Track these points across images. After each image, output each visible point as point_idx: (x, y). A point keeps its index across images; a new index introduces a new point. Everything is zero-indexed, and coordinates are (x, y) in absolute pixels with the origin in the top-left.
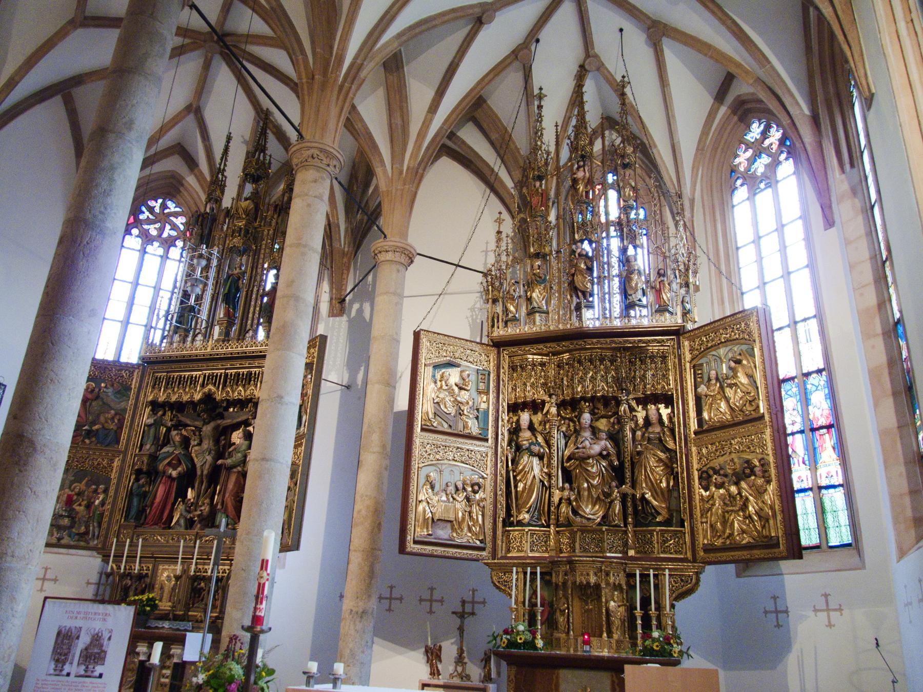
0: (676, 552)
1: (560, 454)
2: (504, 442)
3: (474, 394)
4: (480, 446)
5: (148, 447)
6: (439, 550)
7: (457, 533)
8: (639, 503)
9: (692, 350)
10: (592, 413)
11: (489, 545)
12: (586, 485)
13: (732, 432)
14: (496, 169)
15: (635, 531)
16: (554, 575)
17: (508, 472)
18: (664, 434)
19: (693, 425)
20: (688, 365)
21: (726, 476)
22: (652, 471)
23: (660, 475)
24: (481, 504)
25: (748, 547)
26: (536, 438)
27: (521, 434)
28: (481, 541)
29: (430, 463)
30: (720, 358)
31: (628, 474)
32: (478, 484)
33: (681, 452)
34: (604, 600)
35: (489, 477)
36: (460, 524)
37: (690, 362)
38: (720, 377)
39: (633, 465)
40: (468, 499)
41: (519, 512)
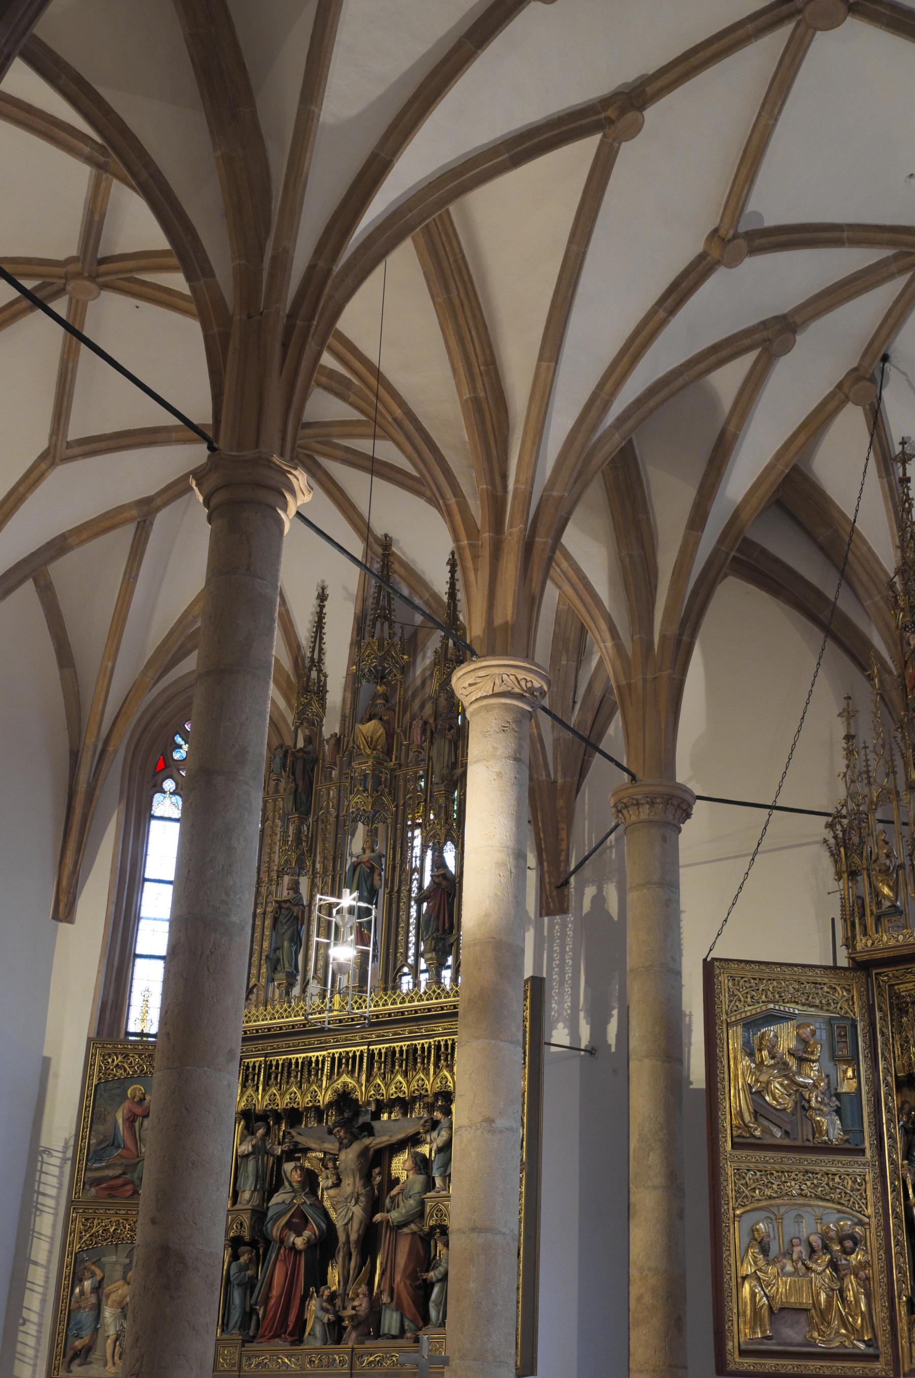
3: (829, 1066)
4: (849, 1164)
5: (246, 1195)
7: (819, 1331)
14: (830, 594)
24: (862, 1274)
28: (868, 1344)
29: (756, 1205)
35: (873, 1221)
36: (824, 1315)
40: (834, 1265)
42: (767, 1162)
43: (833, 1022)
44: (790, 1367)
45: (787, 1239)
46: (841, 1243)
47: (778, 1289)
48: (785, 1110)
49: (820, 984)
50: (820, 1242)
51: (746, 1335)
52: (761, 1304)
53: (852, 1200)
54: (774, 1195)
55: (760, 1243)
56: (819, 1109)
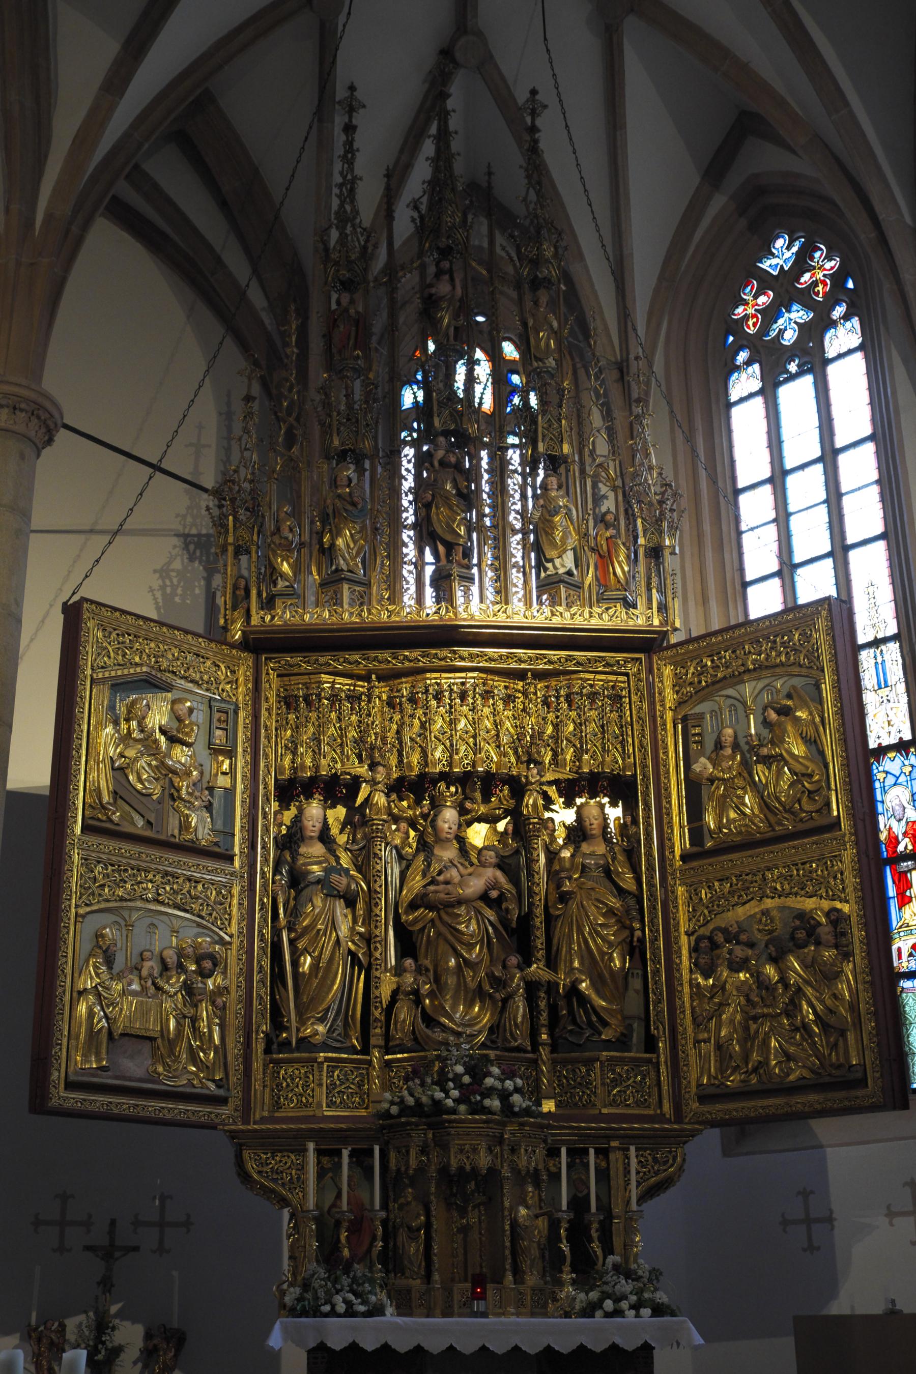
0: (638, 1104)
2: (264, 868)
3: (203, 754)
4: (215, 871)
6: (125, 1105)
7: (164, 1064)
8: (561, 1003)
9: (678, 685)
11: (236, 1093)
12: (452, 962)
13: (766, 854)
15: (554, 1062)
16: (393, 1155)
17: (276, 932)
18: (614, 859)
19: (680, 841)
20: (669, 715)
21: (751, 945)
22: (595, 932)
23: (610, 944)
24: (219, 1001)
25: (798, 1088)
26: (338, 859)
27: (302, 850)
29: (103, 905)
30: (744, 704)
31: (540, 942)
32: (212, 957)
33: (652, 895)
34: (507, 1204)
37: (674, 711)
38: (742, 741)
39: (549, 919)
40: (188, 988)
41: (302, 1021)
42: (122, 856)
43: (213, 703)
44: (124, 1106)
45: (136, 952)
46: (198, 962)
47: (121, 1010)
48: (150, 795)
49: (203, 657)
50: (175, 958)
51: (76, 1064)
52: (99, 1026)
53: (214, 914)
54: (126, 896)
55: (105, 952)
56: (189, 802)
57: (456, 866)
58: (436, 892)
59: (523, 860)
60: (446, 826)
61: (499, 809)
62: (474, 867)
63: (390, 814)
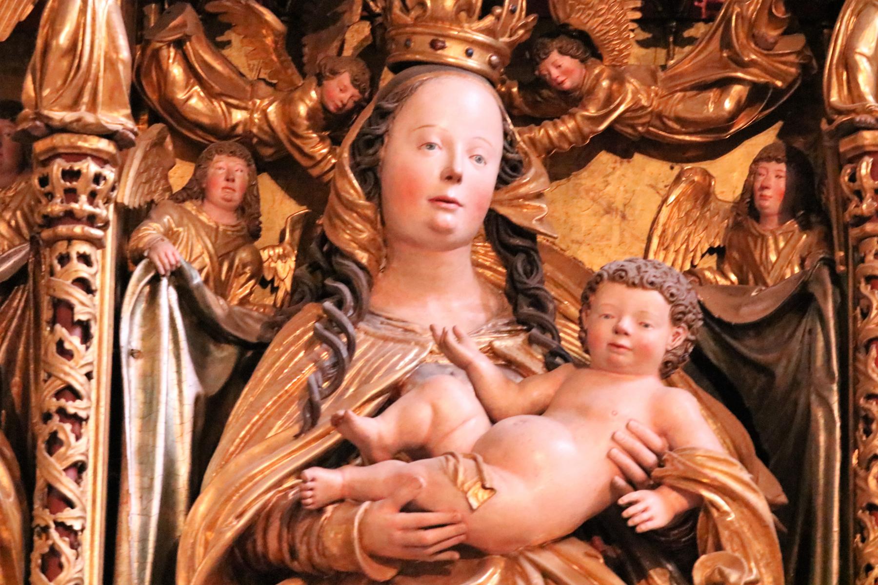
1: (138, 517)
10: (525, 90)
57: (464, 366)
58: (348, 499)
59: (825, 343)
60: (432, 165)
61: (724, 84)
62: (564, 371)
63: (147, 100)
